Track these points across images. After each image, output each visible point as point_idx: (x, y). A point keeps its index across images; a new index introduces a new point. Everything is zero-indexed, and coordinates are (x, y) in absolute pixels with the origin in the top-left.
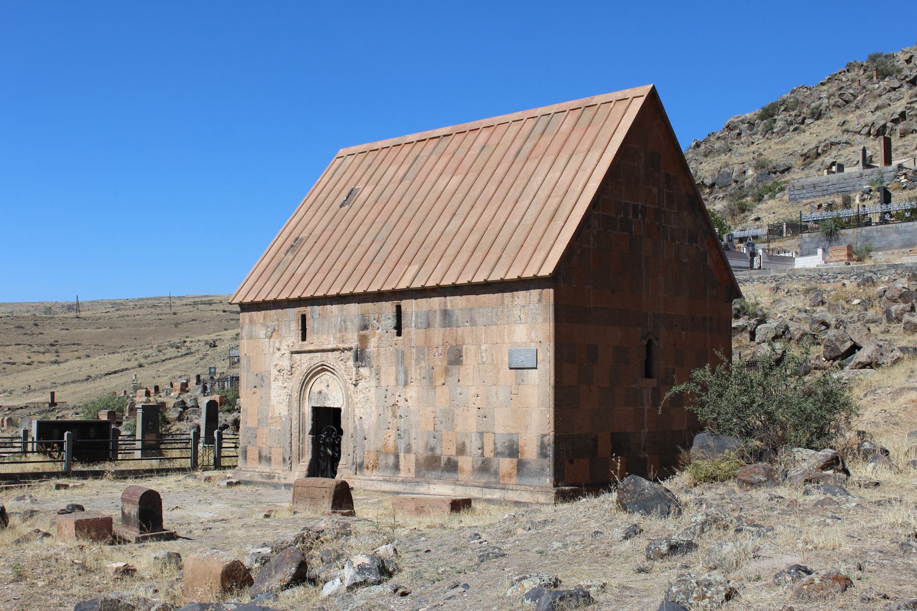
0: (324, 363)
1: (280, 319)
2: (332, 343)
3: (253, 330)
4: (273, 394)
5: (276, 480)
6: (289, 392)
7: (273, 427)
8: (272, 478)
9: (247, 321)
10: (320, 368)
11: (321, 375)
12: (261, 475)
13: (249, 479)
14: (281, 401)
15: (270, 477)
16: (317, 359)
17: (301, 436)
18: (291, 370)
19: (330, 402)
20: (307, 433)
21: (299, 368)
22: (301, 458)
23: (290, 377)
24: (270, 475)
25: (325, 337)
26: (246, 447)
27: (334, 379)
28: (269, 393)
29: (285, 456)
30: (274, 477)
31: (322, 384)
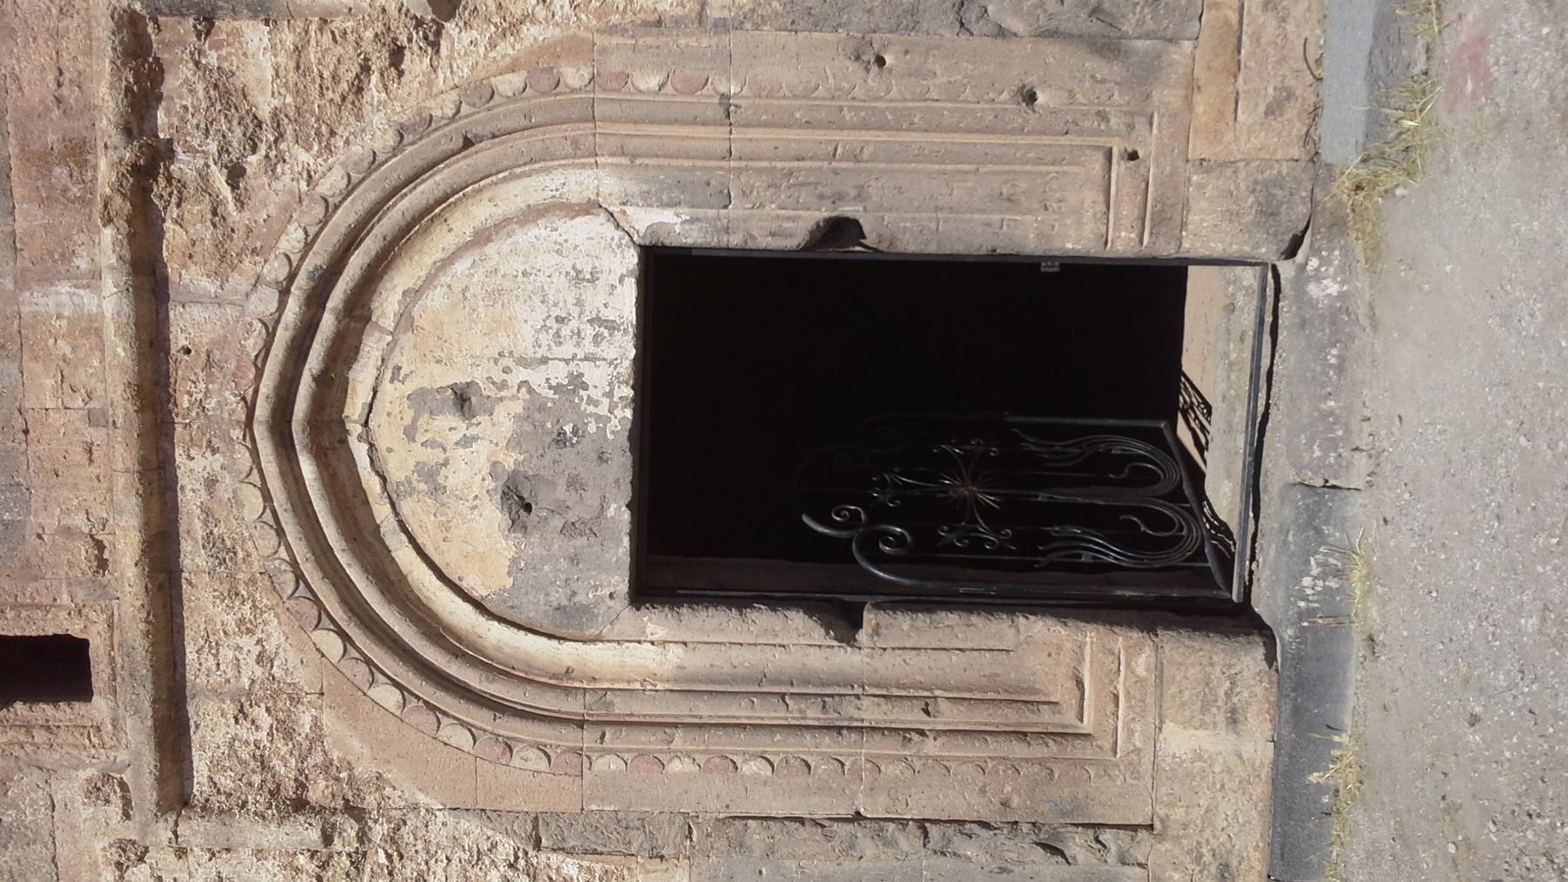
0: (262, 411)
2: (89, 300)
6: (506, 848)
10: (308, 468)
11: (371, 483)
16: (227, 482)
17: (872, 713)
18: (319, 810)
19: (597, 376)
20: (844, 659)
21: (305, 721)
22: (1047, 717)
23: (379, 831)
25: (43, 389)
27: (405, 320)
31: (452, 479)
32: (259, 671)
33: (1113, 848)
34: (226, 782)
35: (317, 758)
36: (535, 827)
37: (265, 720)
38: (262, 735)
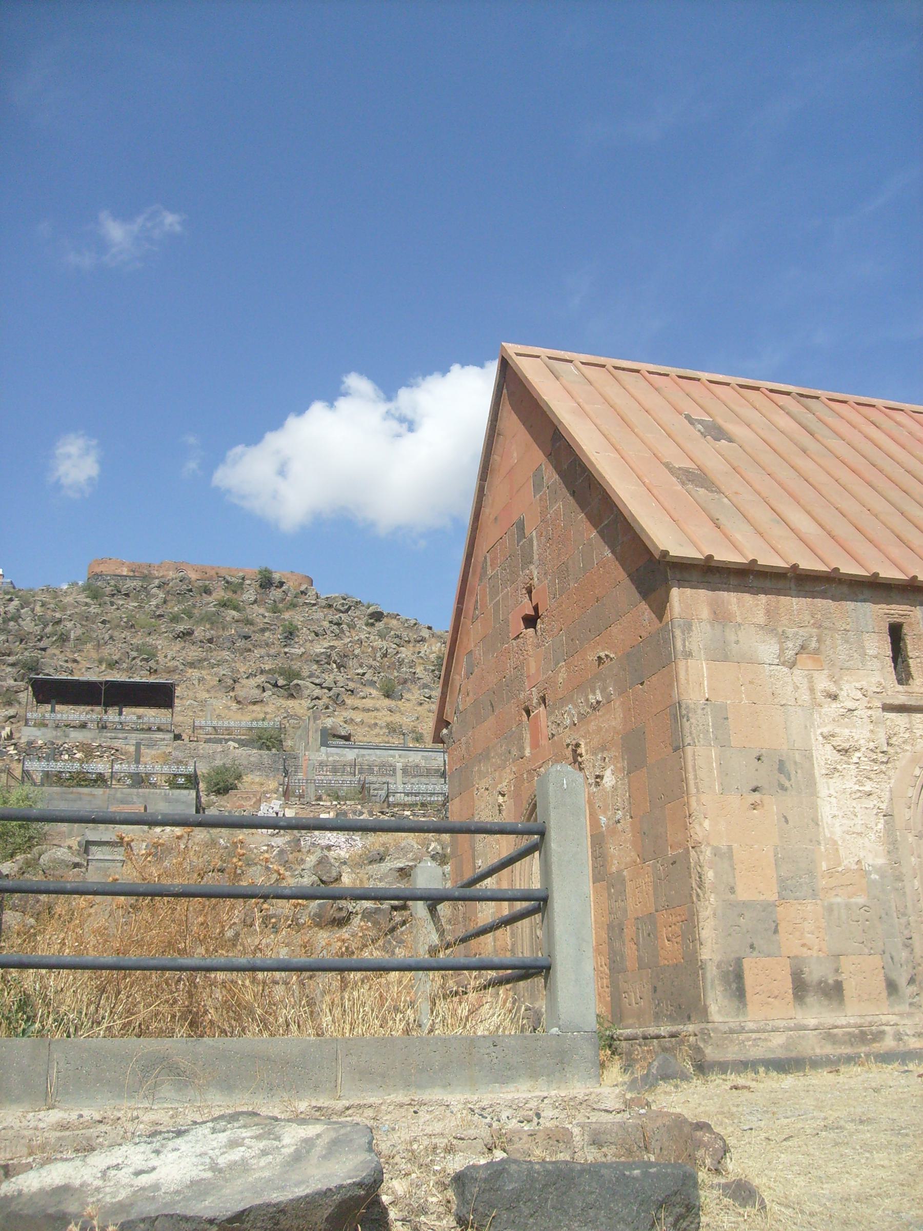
1: (827, 624)
3: (732, 638)
4: (827, 810)
5: (889, 1043)
7: (839, 900)
8: (874, 1040)
9: (705, 613)
12: (829, 1034)
13: (781, 1054)
14: (859, 829)
15: (865, 1036)
23: (883, 767)
24: (863, 1034)
26: (739, 962)
28: (814, 807)
29: (894, 976)
30: (879, 1036)
32: (918, 735)
33: (915, 1000)
34: (888, 723)
35: (899, 751)
36: (890, 815)
37: (907, 735)
38: (902, 735)
